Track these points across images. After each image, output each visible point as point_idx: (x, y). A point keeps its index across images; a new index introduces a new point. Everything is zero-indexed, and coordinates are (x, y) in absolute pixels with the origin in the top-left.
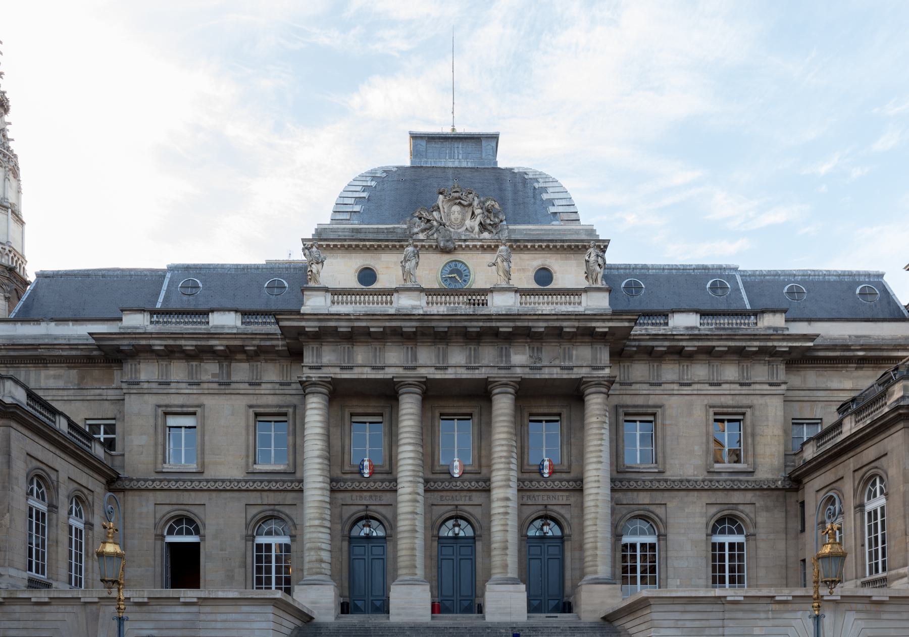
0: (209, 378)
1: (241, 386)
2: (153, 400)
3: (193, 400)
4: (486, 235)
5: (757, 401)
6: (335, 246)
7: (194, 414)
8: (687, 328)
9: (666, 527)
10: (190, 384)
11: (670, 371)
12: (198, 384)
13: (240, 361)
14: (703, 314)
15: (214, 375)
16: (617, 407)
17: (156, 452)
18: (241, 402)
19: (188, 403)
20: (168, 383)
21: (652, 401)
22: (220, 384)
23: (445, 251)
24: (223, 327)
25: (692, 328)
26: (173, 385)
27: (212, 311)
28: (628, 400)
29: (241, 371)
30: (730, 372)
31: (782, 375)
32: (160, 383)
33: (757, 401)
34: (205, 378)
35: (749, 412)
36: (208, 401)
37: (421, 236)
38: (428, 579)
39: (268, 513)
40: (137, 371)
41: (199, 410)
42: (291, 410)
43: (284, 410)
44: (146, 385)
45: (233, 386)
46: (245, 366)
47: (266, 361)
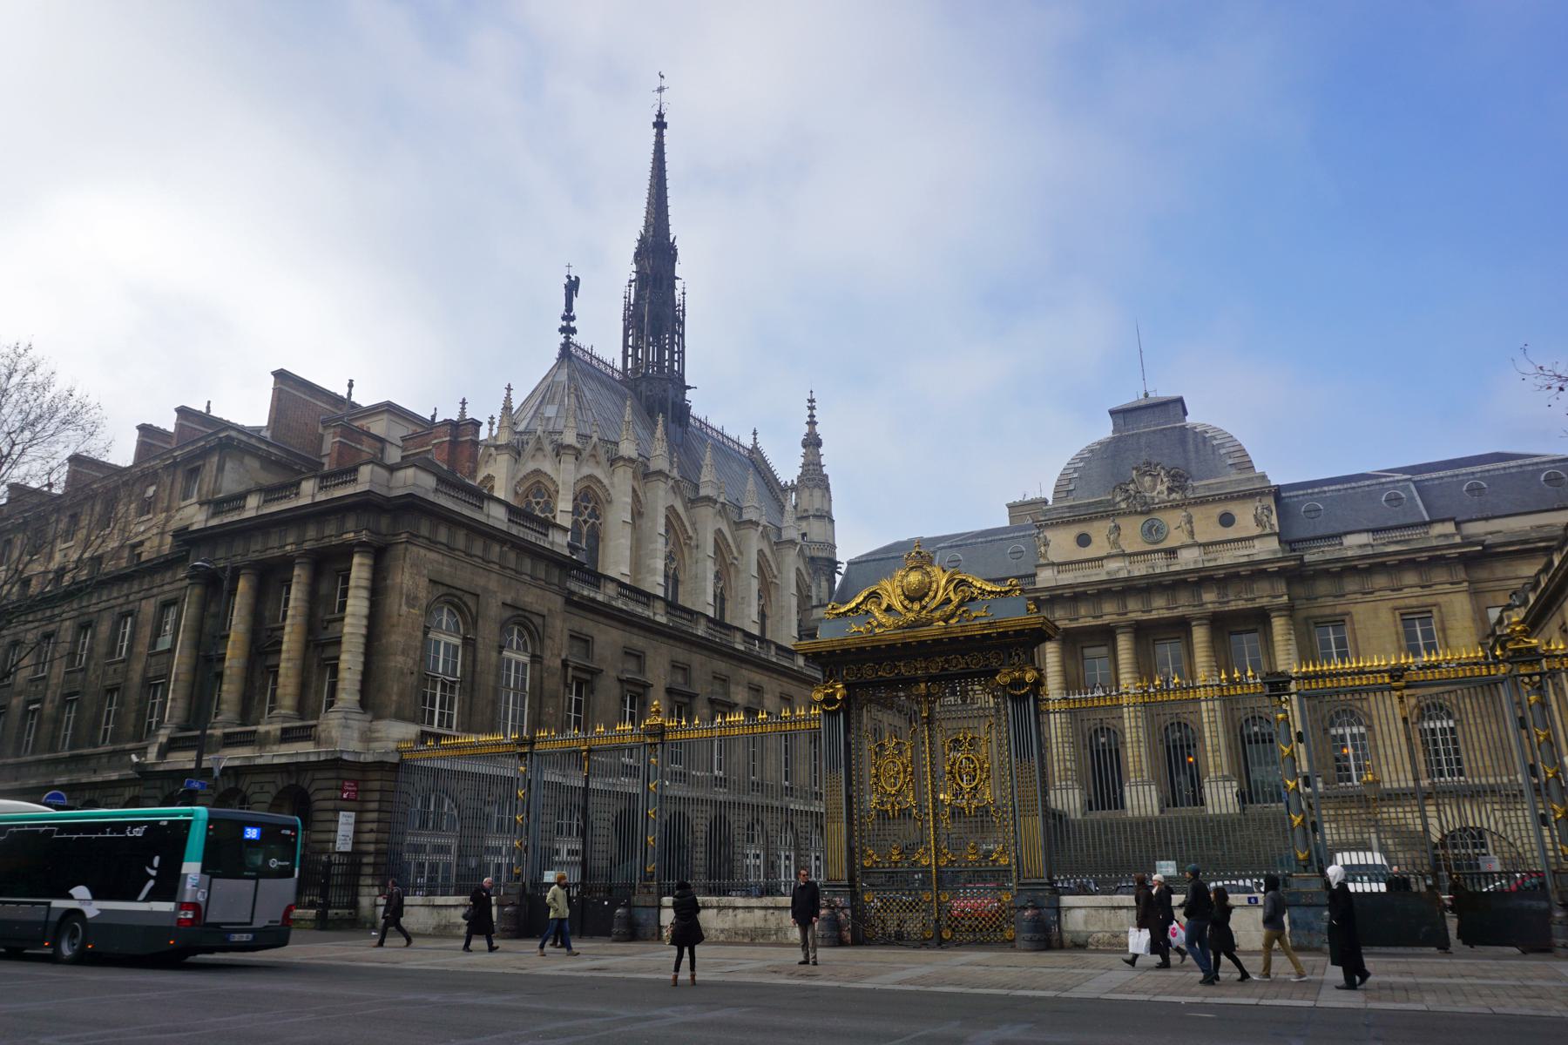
4: (1174, 495)
5: (1440, 599)
8: (1360, 546)
9: (1370, 717)
11: (1351, 585)
14: (1374, 531)
16: (1307, 619)
21: (1339, 610)
23: (1142, 513)
25: (1366, 545)
28: (1316, 612)
30: (1410, 578)
31: (1462, 575)
33: (1440, 599)
35: (1435, 610)
37: (1123, 505)
38: (1155, 778)
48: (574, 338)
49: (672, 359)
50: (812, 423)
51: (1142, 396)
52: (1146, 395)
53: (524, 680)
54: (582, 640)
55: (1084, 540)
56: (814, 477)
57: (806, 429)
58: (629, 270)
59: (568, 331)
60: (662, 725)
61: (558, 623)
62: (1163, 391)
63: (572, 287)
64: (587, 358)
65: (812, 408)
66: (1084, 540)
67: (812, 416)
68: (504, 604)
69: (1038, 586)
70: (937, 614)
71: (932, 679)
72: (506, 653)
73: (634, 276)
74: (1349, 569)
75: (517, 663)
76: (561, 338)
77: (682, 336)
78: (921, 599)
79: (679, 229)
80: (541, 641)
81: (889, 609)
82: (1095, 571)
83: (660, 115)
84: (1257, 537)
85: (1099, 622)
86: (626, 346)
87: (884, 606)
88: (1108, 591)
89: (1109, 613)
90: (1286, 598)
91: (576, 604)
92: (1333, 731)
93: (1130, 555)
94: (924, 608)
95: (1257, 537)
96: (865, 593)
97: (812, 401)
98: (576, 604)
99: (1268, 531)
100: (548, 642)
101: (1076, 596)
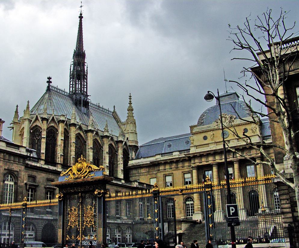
0: (174, 167)
1: (181, 168)
2: (163, 173)
3: (171, 172)
6: (198, 133)
7: (171, 175)
10: (170, 169)
12: (171, 169)
13: (180, 162)
15: (175, 166)
17: (164, 185)
18: (181, 171)
19: (170, 173)
20: (165, 169)
22: (176, 168)
24: (175, 155)
26: (167, 170)
27: (173, 152)
29: (180, 165)
32: (164, 170)
34: (173, 167)
36: (174, 172)
37: (216, 127)
39: (188, 196)
40: (159, 167)
41: (172, 174)
42: (191, 172)
43: (190, 172)
44: (161, 170)
45: (179, 168)
46: (181, 163)
47: (185, 162)
48: (51, 84)
49: (84, 88)
50: (130, 103)
52: (227, 92)
53: (12, 189)
54: (34, 178)
55: (205, 138)
56: (131, 120)
59: (49, 82)
60: (26, 204)
61: (23, 173)
65: (130, 99)
66: (205, 138)
68: (5, 169)
69: (190, 153)
70: (82, 176)
71: (82, 192)
72: (6, 182)
73: (73, 63)
75: (10, 185)
76: (47, 84)
77: (87, 79)
78: (80, 171)
79: (86, 48)
80: (17, 178)
81: (74, 174)
82: (207, 148)
83: (81, 14)
84: (252, 136)
85: (208, 163)
86: (70, 84)
87: (73, 173)
88: (210, 154)
89: (211, 160)
90: (260, 154)
91: (27, 167)
93: (216, 143)
94: (81, 173)
95: (252, 136)
96: (69, 170)
97: (130, 96)
98: (27, 167)
99: (255, 134)
100: (20, 179)
101: (201, 156)
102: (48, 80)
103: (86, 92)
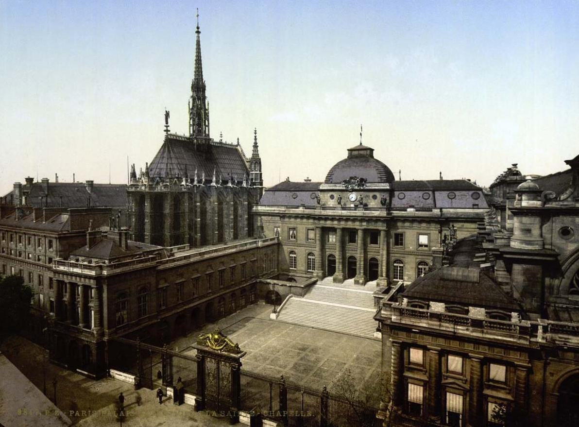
11: (407, 224)
30: (424, 225)
50: (256, 139)
51: (359, 144)
52: (361, 144)
57: (254, 141)
58: (189, 93)
59: (167, 131)
62: (366, 144)
63: (167, 115)
64: (175, 138)
65: (255, 133)
67: (255, 137)
74: (405, 219)
83: (198, 28)
92: (395, 265)
102: (165, 128)
103: (209, 135)
